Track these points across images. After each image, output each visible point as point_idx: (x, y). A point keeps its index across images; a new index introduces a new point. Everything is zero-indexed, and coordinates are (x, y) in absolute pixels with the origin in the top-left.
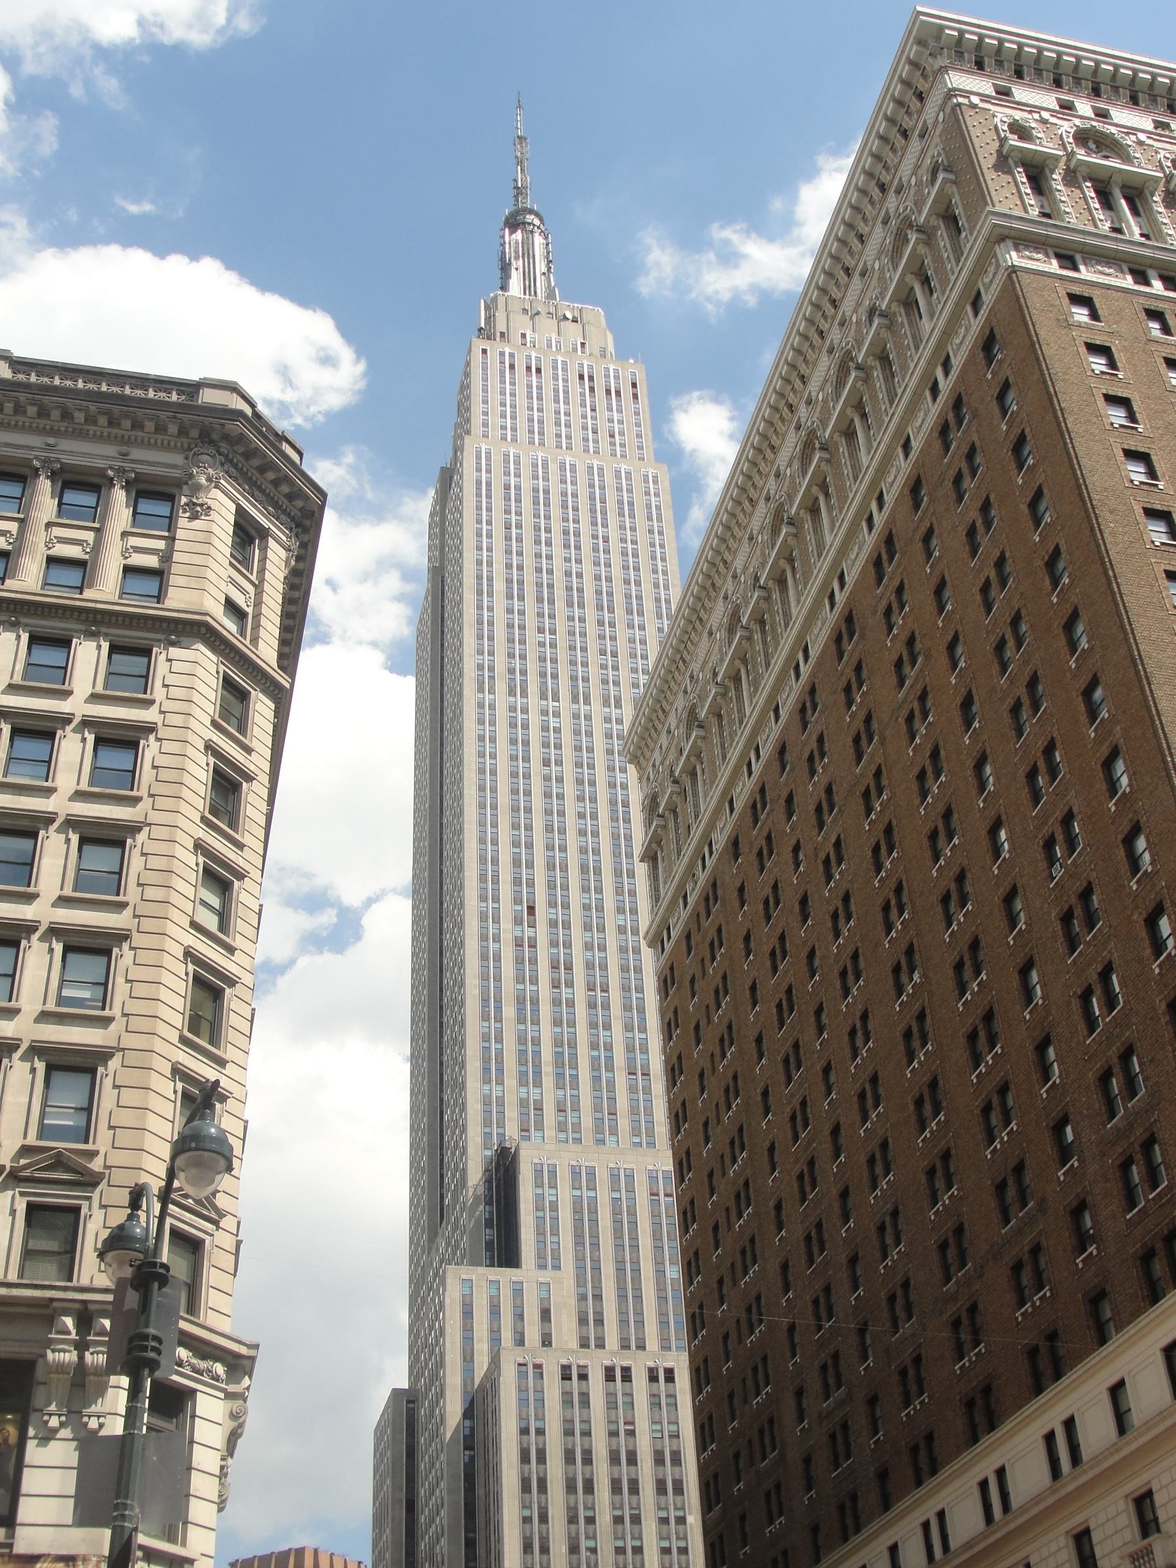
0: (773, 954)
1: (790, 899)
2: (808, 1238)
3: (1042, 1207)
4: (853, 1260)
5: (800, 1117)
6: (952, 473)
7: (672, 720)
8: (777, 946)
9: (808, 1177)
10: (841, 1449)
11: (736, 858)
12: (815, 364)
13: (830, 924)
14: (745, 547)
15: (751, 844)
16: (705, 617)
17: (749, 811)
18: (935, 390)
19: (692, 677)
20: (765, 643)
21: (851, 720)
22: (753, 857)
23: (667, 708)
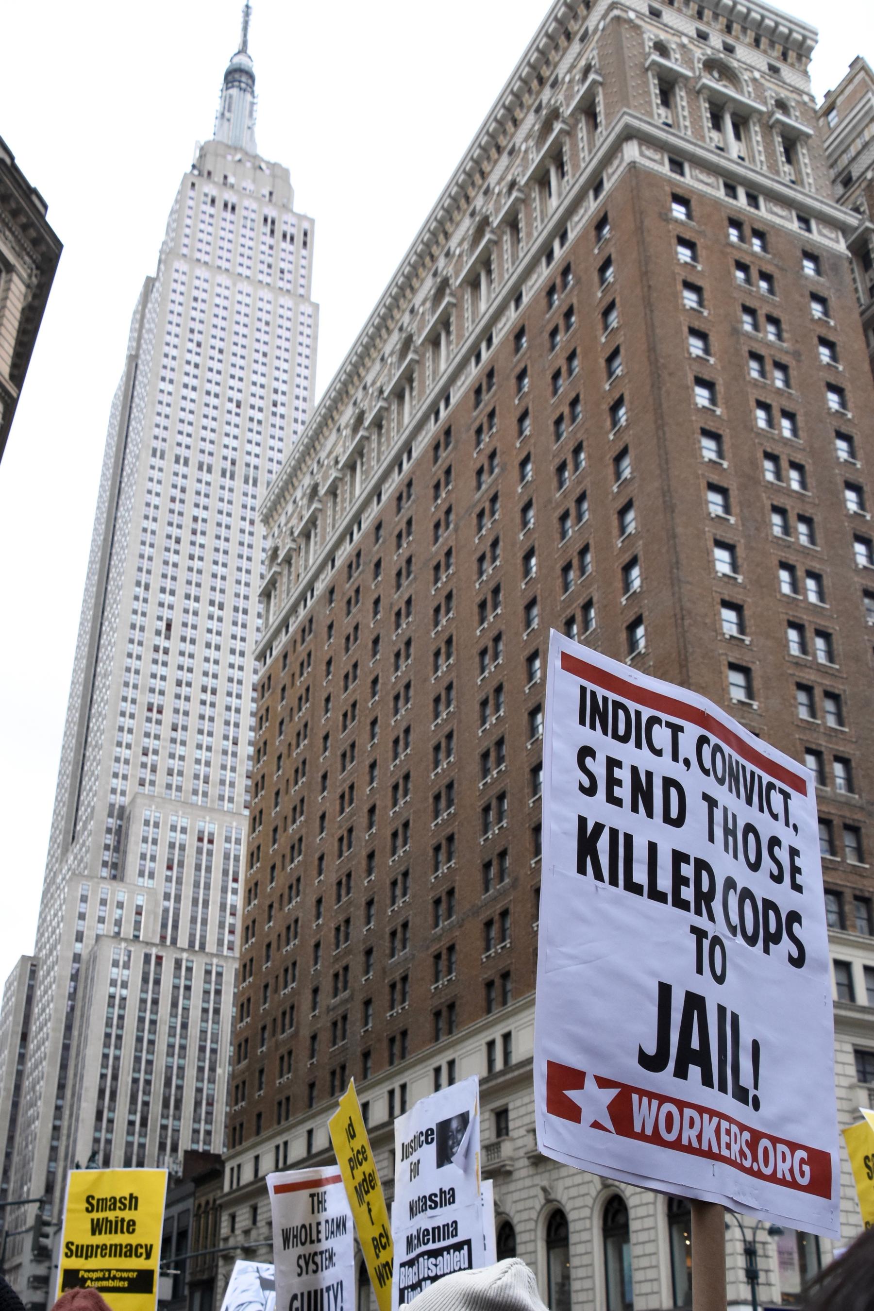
0: (346, 677)
1: (365, 638)
2: (339, 884)
4: (370, 903)
5: (346, 797)
7: (299, 494)
8: (351, 671)
9: (346, 839)
10: (339, 1033)
11: (331, 602)
12: (458, 224)
13: (392, 660)
14: (377, 366)
15: (344, 594)
16: (336, 418)
17: (346, 570)
19: (319, 462)
20: (379, 443)
23: (296, 483)
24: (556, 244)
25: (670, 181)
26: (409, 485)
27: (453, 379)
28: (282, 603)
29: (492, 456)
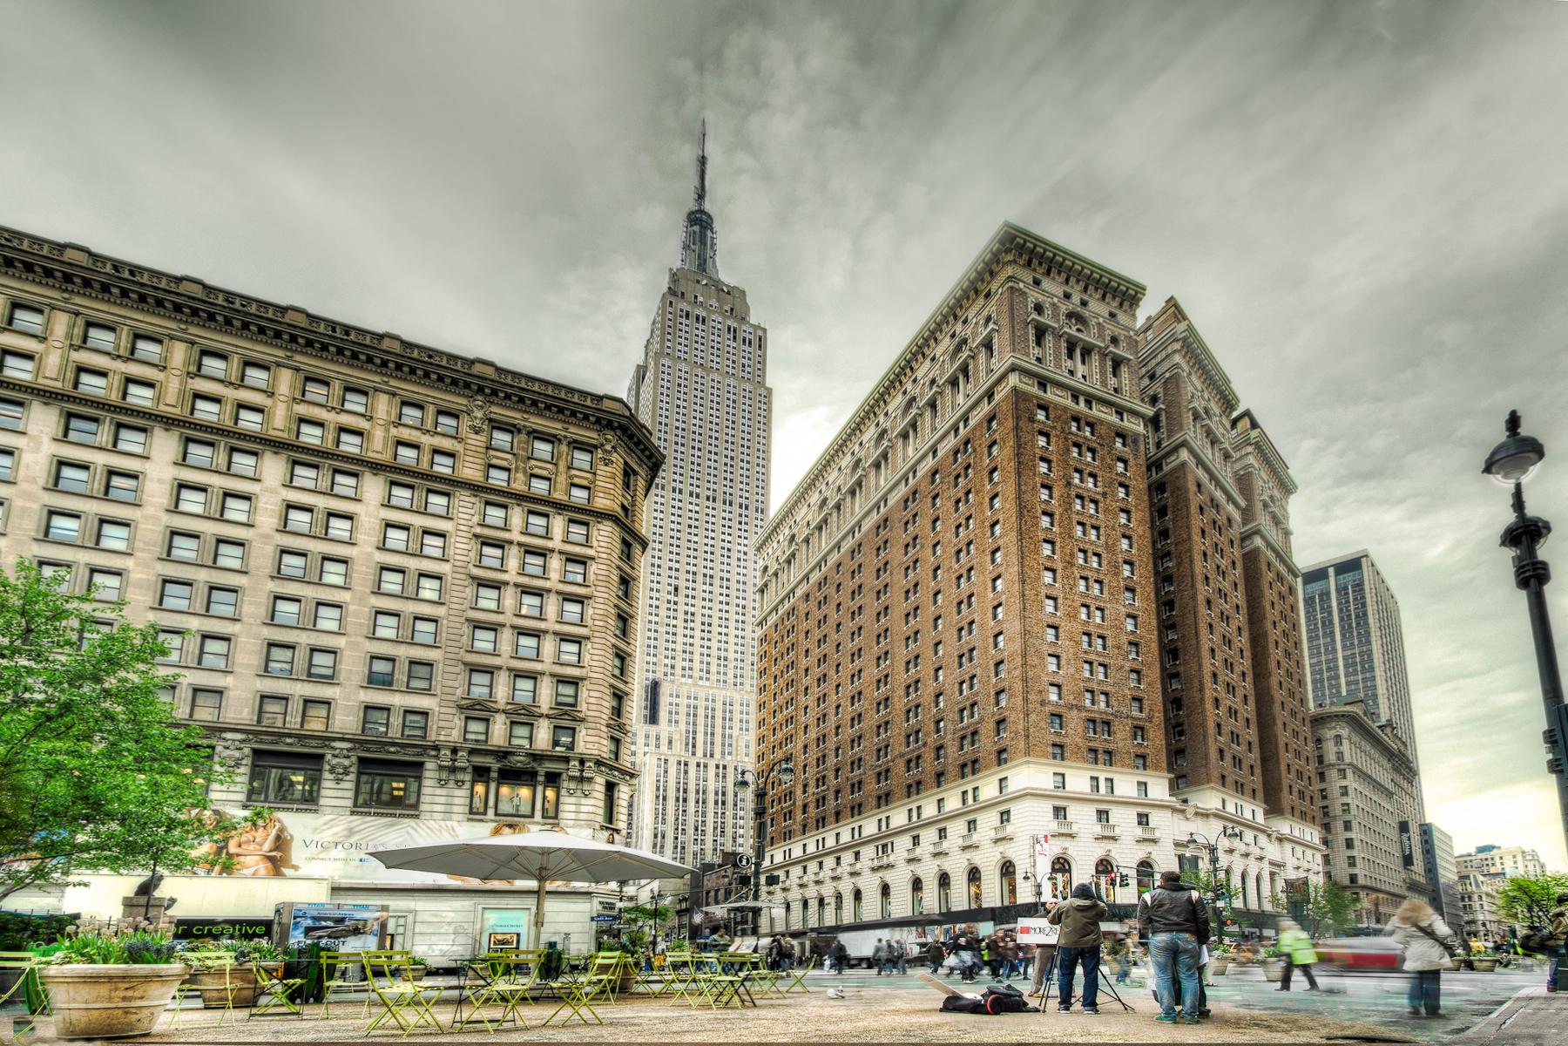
3: (925, 745)
6: (955, 473)
18: (957, 431)
21: (877, 562)
22: (816, 603)
24: (961, 425)
25: (1037, 397)
26: (860, 545)
27: (891, 490)
28: (772, 597)
29: (915, 538)
